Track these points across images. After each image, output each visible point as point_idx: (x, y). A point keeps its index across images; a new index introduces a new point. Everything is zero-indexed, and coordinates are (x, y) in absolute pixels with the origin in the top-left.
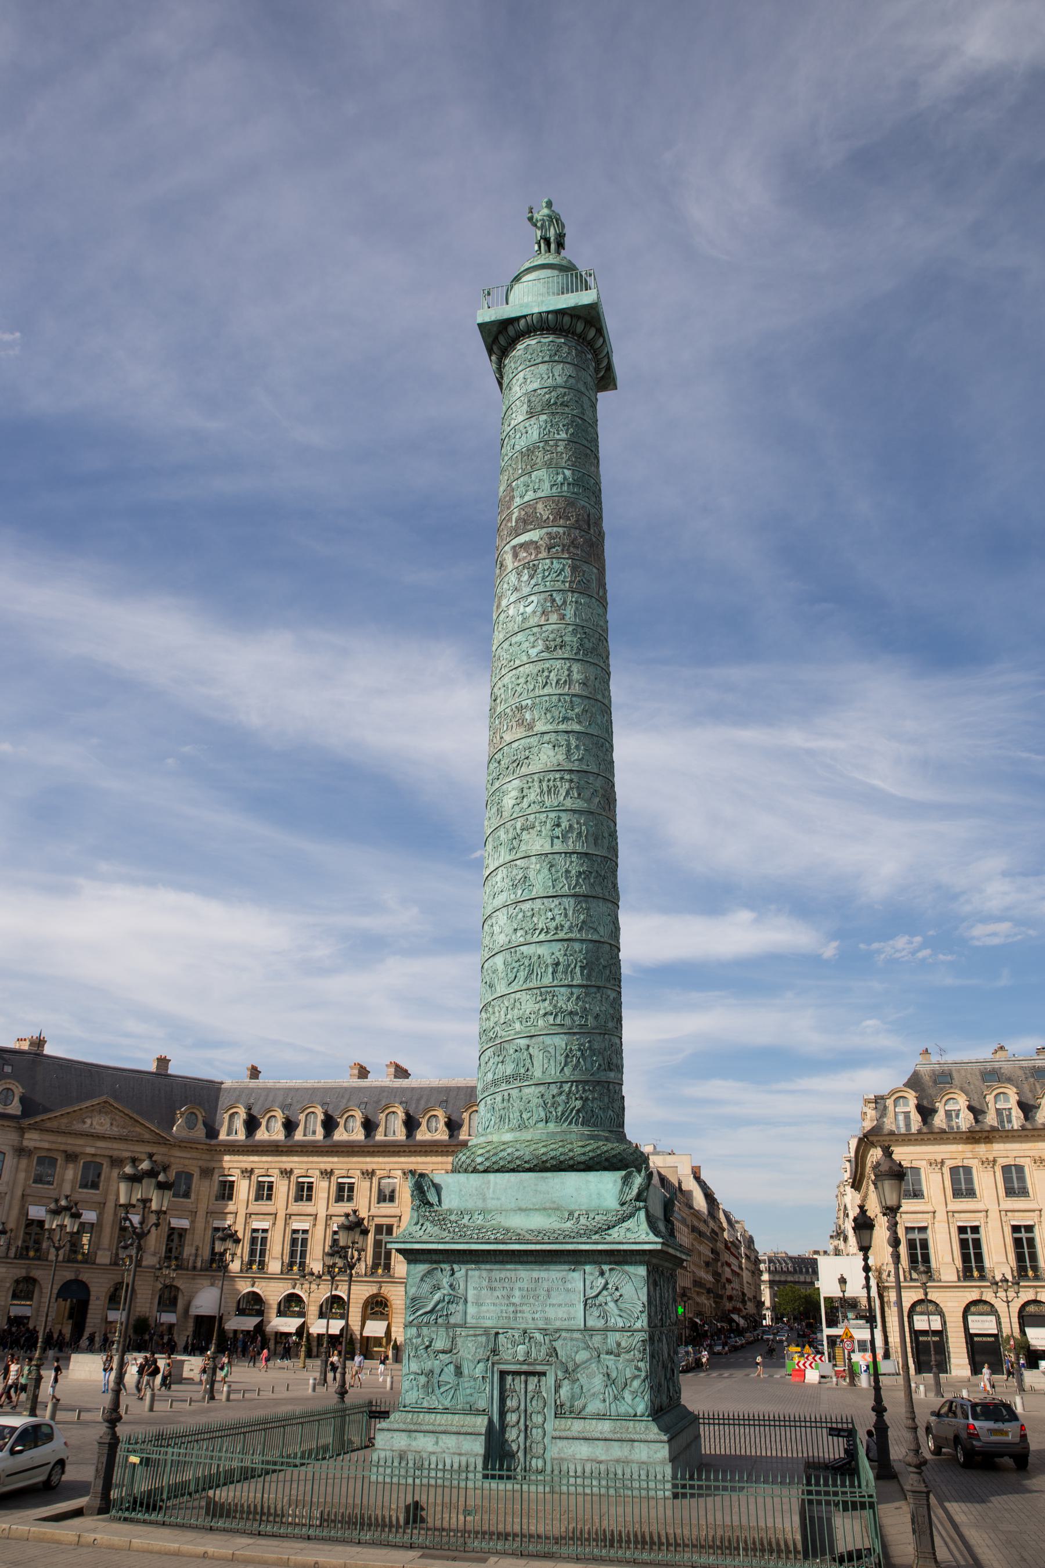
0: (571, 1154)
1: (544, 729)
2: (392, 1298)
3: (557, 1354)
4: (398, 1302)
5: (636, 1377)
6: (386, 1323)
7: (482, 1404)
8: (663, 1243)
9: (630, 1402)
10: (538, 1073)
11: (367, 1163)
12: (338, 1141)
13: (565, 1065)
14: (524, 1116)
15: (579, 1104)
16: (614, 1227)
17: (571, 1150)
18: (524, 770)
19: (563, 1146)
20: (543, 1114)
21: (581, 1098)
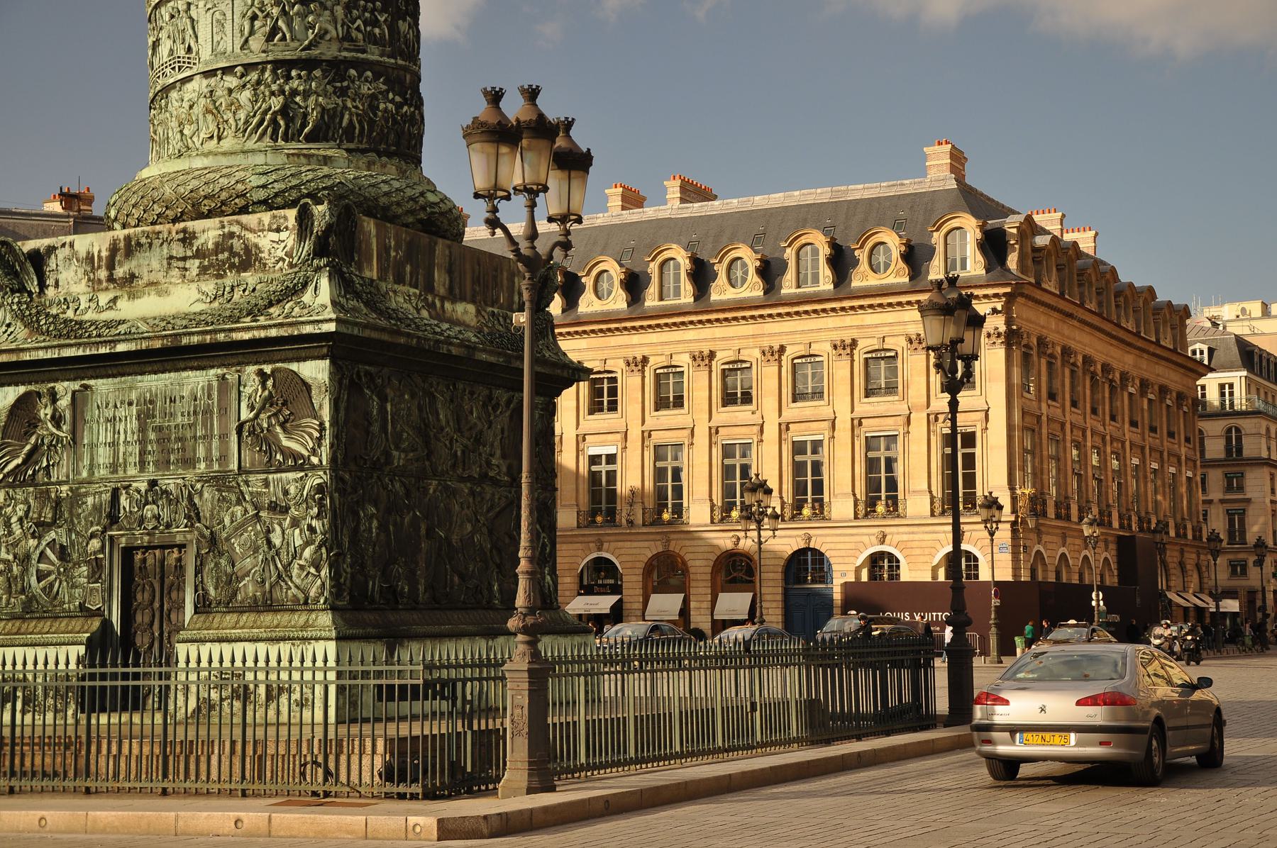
0: (240, 187)
2: (687, 557)
3: (198, 514)
4: (698, 563)
5: (307, 543)
6: (679, 597)
7: (95, 604)
8: (338, 320)
9: (298, 581)
10: (206, 54)
11: (633, 346)
12: (587, 315)
13: (252, 33)
14: (186, 132)
15: (276, 103)
16: (279, 301)
17: (242, 181)
19: (228, 176)
20: (213, 127)
21: (282, 92)
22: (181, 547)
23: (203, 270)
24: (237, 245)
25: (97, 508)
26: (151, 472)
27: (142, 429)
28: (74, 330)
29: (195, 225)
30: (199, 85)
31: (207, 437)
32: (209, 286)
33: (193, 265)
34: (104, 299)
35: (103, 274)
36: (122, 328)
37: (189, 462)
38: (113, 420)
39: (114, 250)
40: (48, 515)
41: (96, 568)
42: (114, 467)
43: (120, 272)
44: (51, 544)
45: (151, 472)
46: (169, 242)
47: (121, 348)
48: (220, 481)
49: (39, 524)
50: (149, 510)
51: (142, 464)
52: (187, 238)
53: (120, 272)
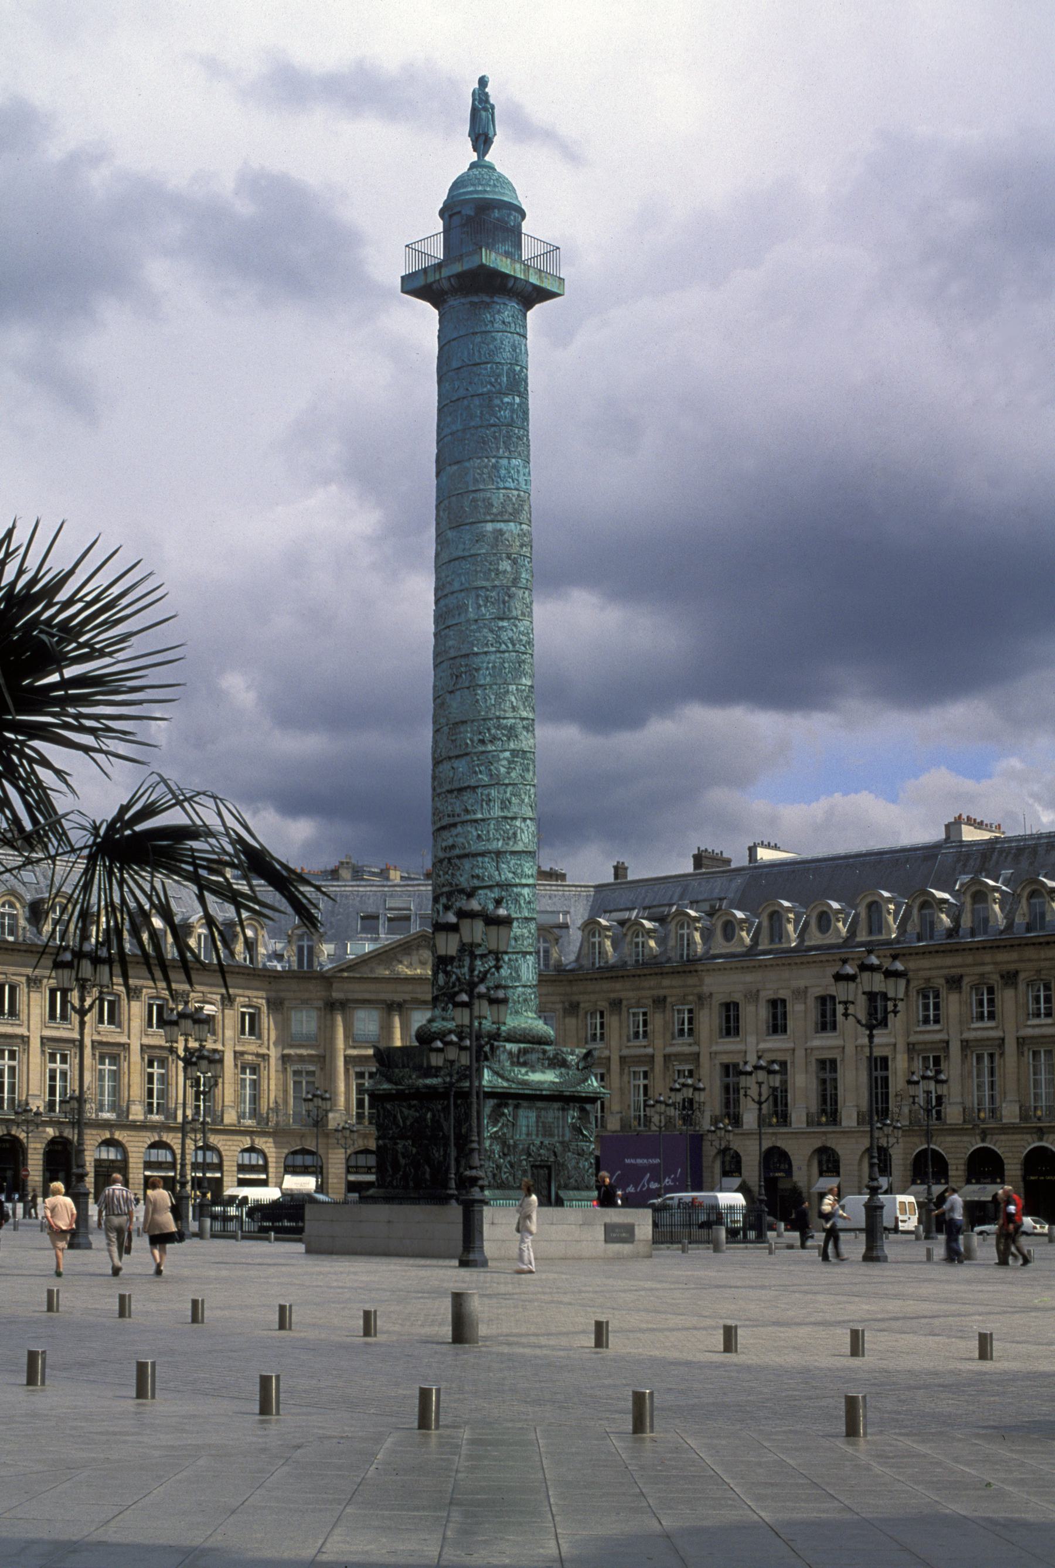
1: (525, 714)
18: (512, 746)
22: (549, 1168)
23: (549, 1065)
24: (560, 1057)
25: (523, 1149)
26: (540, 1139)
27: (537, 1122)
28: (525, 1083)
29: (547, 1048)
30: (520, 989)
31: (558, 1127)
32: (557, 1072)
33: (546, 1062)
34: (523, 1070)
35: (515, 1060)
36: (546, 1086)
37: (552, 1135)
38: (527, 1117)
39: (519, 1050)
40: (506, 1151)
41: (525, 1172)
42: (528, 1135)
43: (521, 1060)
44: (509, 1162)
45: (540, 1139)
46: (538, 1051)
47: (544, 1093)
48: (562, 1143)
49: (504, 1155)
50: (542, 1151)
51: (537, 1135)
52: (544, 1052)
53: (521, 1060)
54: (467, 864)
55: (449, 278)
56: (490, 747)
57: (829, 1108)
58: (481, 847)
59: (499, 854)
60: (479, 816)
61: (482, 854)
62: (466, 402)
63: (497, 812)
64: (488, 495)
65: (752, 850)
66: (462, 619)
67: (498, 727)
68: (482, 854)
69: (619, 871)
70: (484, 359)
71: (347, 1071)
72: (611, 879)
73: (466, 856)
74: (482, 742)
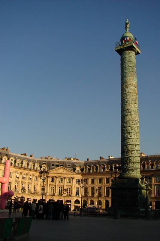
54: (130, 146)
55: (125, 47)
56: (134, 125)
57: (100, 194)
58: (133, 143)
59: (136, 144)
60: (132, 137)
61: (133, 144)
62: (128, 67)
63: (135, 137)
64: (132, 83)
65: (109, 157)
66: (129, 103)
67: (135, 122)
68: (133, 144)
69: (88, 159)
70: (131, 61)
71: (49, 186)
72: (87, 160)
73: (130, 144)
74: (133, 124)
